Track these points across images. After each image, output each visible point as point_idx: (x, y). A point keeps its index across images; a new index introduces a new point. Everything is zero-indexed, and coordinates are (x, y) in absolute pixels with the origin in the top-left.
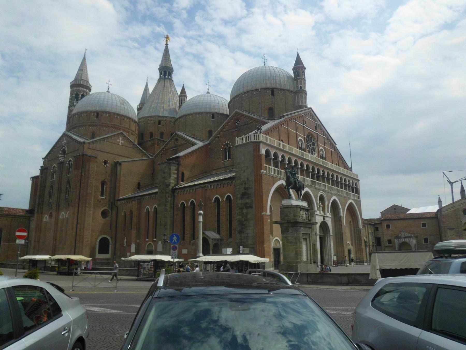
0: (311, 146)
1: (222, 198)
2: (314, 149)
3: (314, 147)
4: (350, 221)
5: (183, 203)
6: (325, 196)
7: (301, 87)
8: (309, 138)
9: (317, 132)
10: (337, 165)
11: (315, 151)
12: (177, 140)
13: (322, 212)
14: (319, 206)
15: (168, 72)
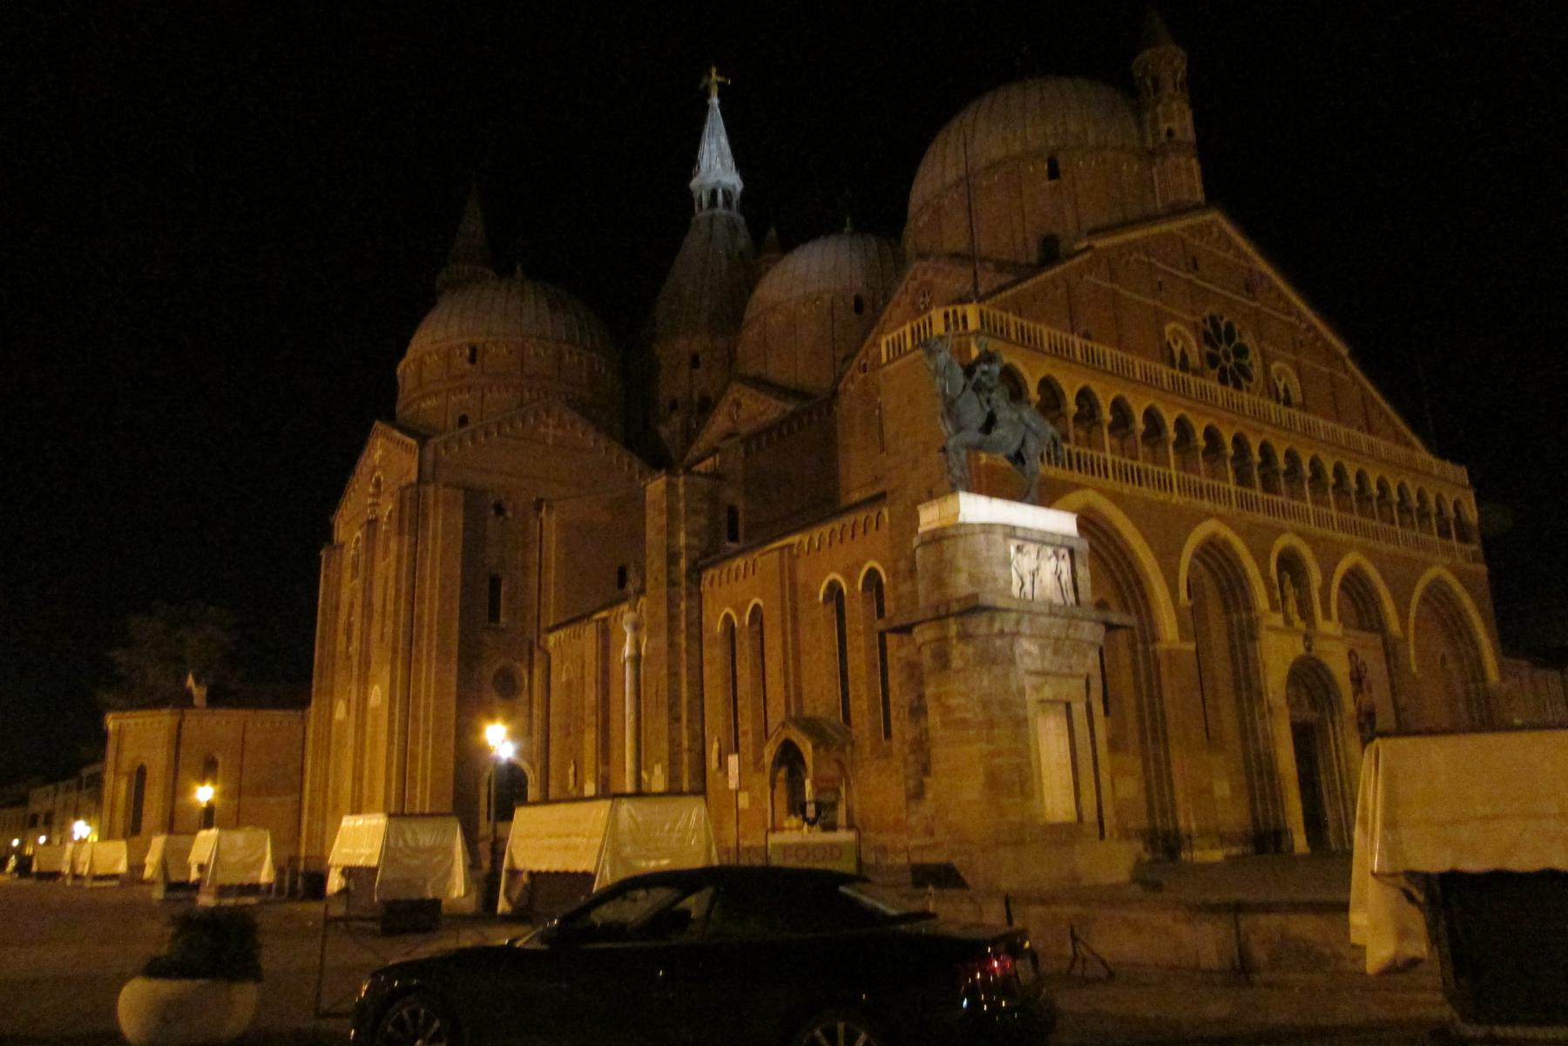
0: (1227, 357)
1: (850, 577)
2: (1245, 372)
3: (1246, 363)
4: (1443, 659)
5: (728, 617)
6: (1306, 551)
7: (1170, 133)
8: (1216, 326)
9: (1254, 299)
10: (1359, 428)
11: (1250, 378)
12: (739, 405)
13: (1296, 618)
14: (1278, 596)
15: (720, 190)
